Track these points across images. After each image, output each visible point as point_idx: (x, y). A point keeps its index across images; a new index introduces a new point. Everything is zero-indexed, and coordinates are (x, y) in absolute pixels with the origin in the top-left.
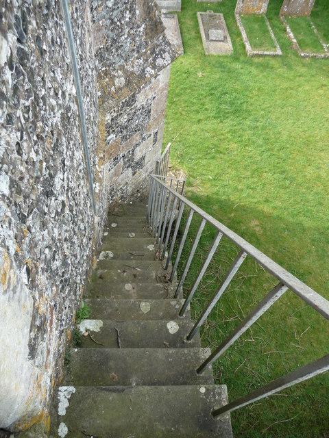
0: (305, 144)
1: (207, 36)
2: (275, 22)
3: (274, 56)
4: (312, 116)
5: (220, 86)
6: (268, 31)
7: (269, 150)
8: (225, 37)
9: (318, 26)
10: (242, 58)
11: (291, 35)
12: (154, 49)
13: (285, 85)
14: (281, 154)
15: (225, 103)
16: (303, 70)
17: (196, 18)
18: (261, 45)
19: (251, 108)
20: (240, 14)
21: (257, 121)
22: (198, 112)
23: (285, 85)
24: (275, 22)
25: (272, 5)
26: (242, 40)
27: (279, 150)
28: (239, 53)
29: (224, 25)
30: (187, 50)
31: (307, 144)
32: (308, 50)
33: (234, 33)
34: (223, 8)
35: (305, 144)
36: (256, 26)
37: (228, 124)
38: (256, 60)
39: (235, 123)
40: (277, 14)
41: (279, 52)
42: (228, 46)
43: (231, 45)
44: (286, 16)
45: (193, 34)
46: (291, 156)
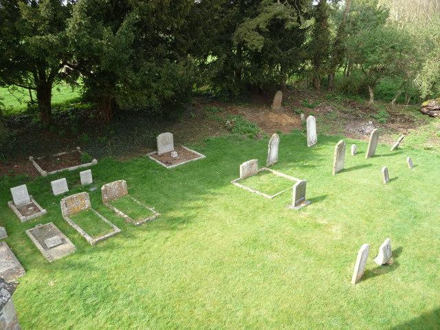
0: (180, 292)
1: (45, 246)
2: (103, 210)
3: (115, 235)
4: (172, 266)
5: (77, 283)
6: (100, 219)
7: (153, 316)
8: (63, 240)
9: (138, 198)
10: (87, 249)
11: (121, 213)
12: (216, 98)
13: (137, 253)
14: (166, 313)
15: (90, 296)
16: (145, 234)
17: (27, 235)
18: (99, 232)
19: (116, 288)
20: (69, 216)
21: (128, 297)
22: (64, 321)
23: (137, 253)
24: (103, 210)
25: (93, 200)
26: (80, 235)
27: (162, 311)
28: (82, 247)
29: (58, 230)
30: (28, 267)
31: (182, 291)
32: (140, 218)
33: (67, 231)
34: (50, 218)
35: (180, 292)
36: (88, 219)
37: (102, 314)
38: (101, 245)
39: (108, 310)
40: (101, 203)
41: (118, 230)
42: (69, 245)
43: (72, 244)
44: (109, 201)
45: (29, 250)
46: (175, 310)
